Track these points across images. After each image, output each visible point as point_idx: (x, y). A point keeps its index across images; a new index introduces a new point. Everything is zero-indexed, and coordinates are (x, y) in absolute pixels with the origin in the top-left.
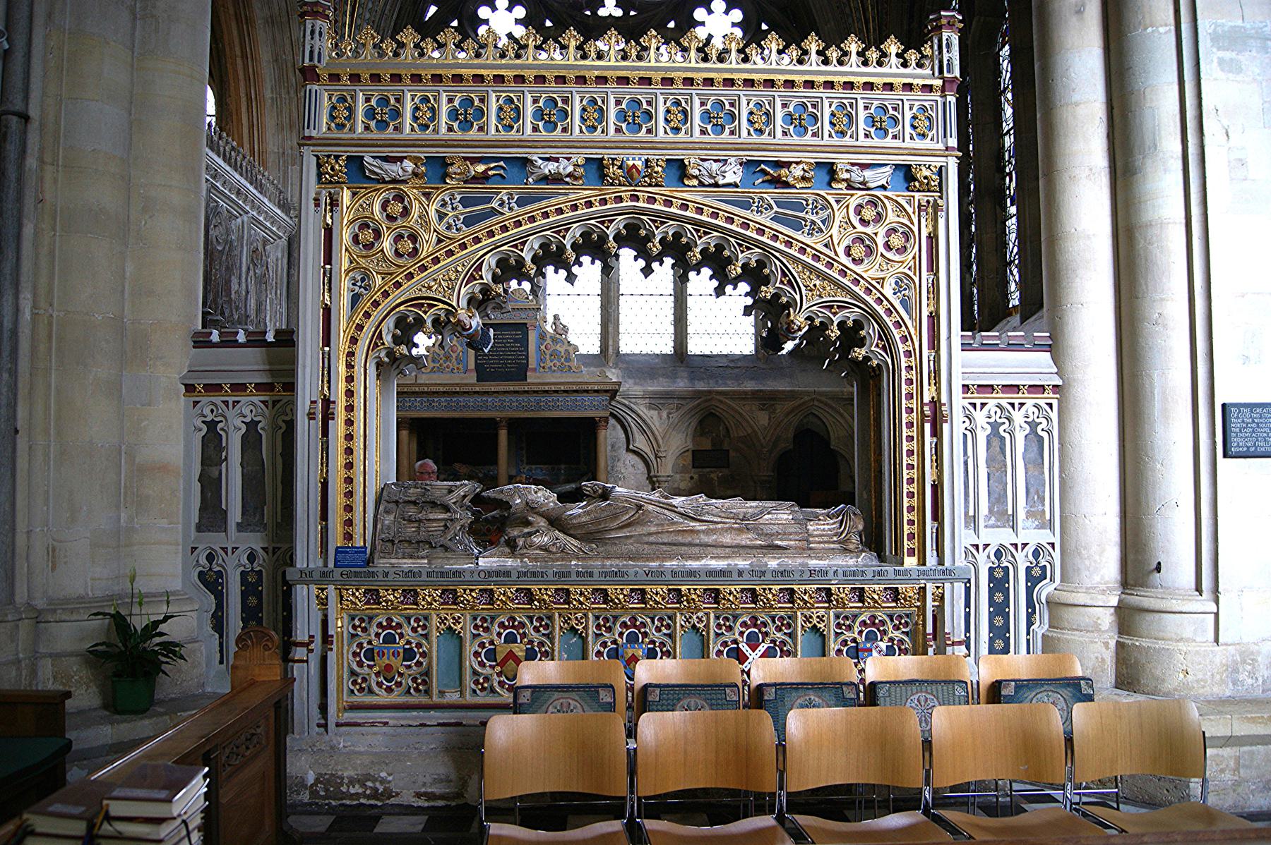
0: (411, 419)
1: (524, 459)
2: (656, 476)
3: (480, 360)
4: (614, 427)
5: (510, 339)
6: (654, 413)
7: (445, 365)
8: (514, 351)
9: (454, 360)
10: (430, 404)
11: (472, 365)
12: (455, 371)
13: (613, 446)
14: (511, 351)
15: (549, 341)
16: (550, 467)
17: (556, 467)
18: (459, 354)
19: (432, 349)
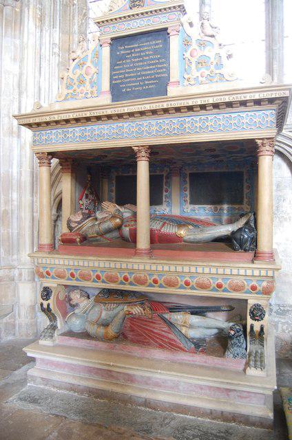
1: (188, 199)
3: (116, 80)
4: (279, 166)
9: (88, 83)
11: (106, 85)
12: (89, 95)
13: (278, 186)
14: (149, 65)
15: (194, 45)
16: (212, 207)
17: (219, 207)
18: (93, 76)
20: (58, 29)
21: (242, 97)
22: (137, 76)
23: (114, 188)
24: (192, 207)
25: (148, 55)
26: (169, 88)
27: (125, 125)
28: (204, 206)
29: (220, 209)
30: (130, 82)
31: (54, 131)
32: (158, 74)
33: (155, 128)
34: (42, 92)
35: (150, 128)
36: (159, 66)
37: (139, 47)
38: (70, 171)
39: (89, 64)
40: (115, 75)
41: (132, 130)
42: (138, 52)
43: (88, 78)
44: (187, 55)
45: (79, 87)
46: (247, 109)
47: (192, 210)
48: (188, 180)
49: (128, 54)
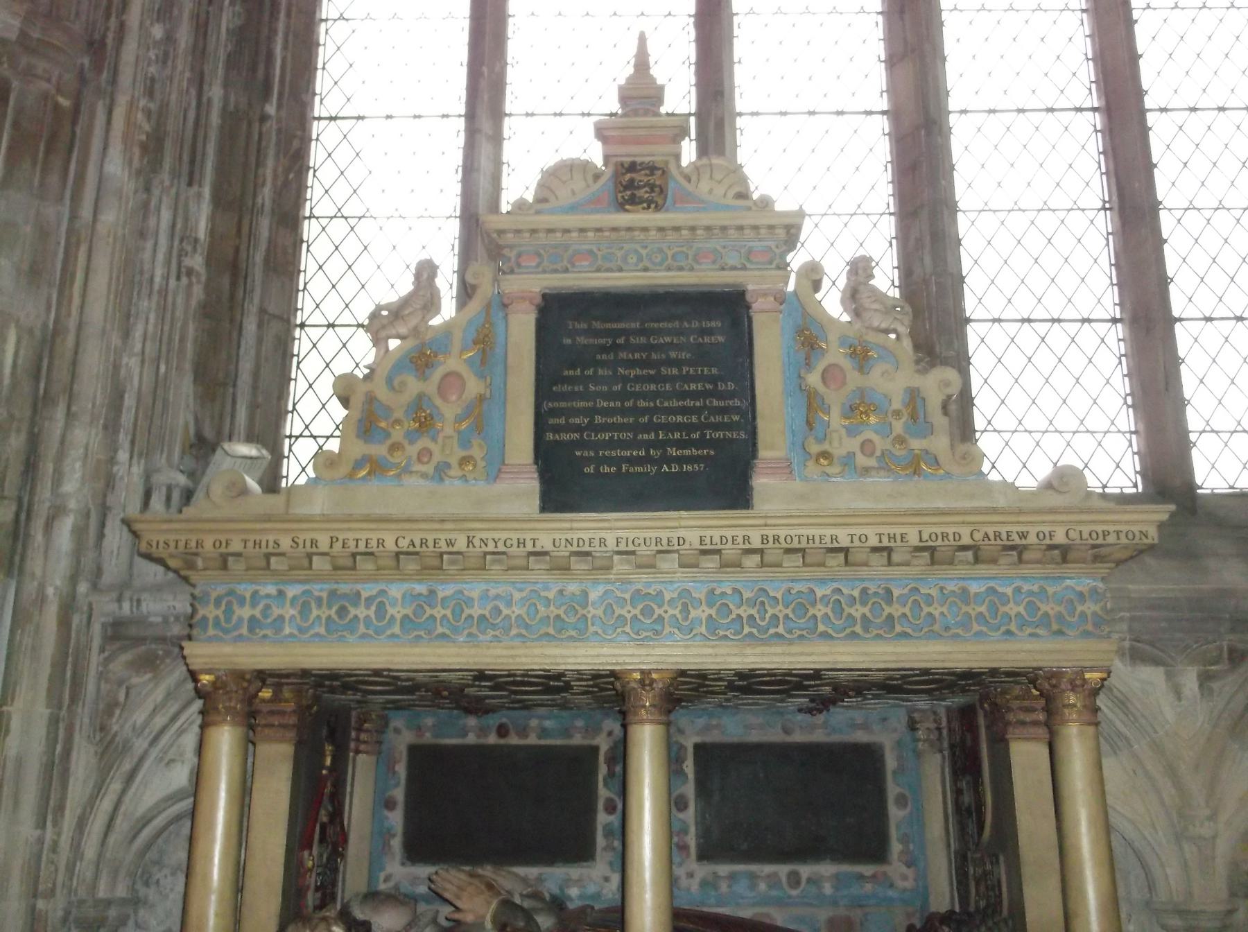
0: (262, 676)
2: (1181, 913)
3: (557, 429)
5: (679, 347)
6: (1153, 675)
7: (413, 450)
8: (695, 395)
10: (342, 611)
12: (455, 472)
14: (684, 395)
15: (835, 355)
17: (805, 870)
19: (363, 389)
20: (207, 191)
21: (1015, 537)
22: (636, 428)
23: (399, 794)
24: (703, 870)
25: (678, 363)
26: (761, 482)
27: (594, 595)
28: (753, 868)
29: (809, 880)
30: (611, 444)
31: (292, 591)
32: (716, 427)
33: (701, 613)
34: (129, 401)
35: (685, 610)
36: (716, 403)
37: (642, 332)
38: (292, 734)
39: (453, 363)
40: (554, 413)
41: (618, 611)
42: (641, 348)
43: (449, 410)
44: (814, 379)
45: (411, 437)
46: (1025, 570)
47: (704, 884)
48: (689, 767)
49: (604, 349)
